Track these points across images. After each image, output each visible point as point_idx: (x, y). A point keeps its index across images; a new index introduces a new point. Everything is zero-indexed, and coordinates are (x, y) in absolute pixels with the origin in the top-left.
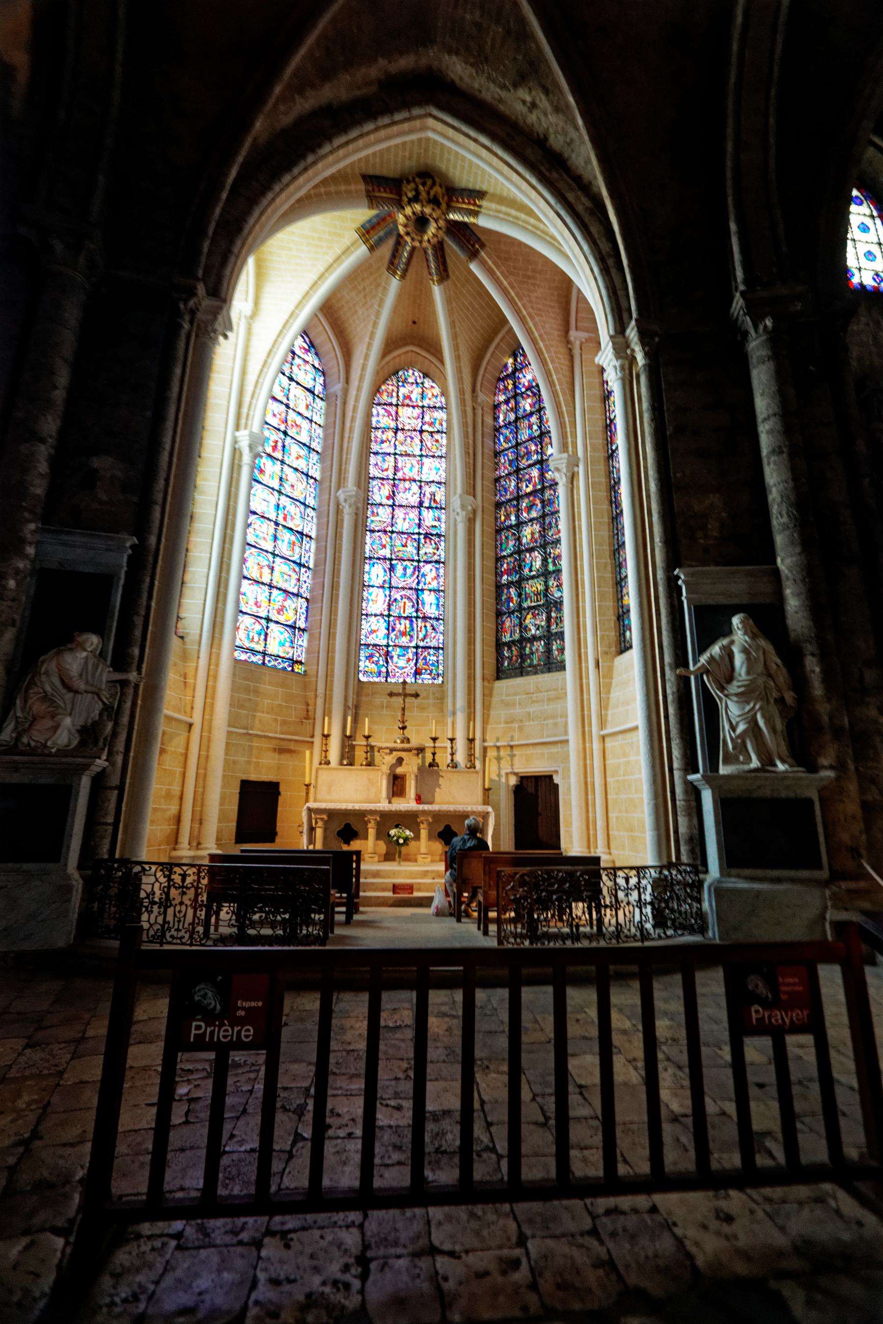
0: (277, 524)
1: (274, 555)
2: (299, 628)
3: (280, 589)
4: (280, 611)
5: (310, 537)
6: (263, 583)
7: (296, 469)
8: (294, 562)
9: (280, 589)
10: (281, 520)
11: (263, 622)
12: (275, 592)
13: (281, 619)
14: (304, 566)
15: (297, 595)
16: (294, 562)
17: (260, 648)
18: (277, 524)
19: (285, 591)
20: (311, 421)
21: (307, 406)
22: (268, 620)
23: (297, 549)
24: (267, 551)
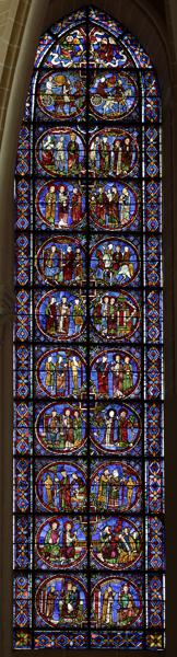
0: (88, 401)
1: (88, 458)
2: (151, 571)
3: (107, 514)
4: (111, 549)
5: (158, 401)
6: (72, 514)
7: (116, 288)
8: (129, 458)
9: (107, 514)
10: (94, 392)
11: (83, 578)
12: (98, 523)
13: (111, 563)
14: (150, 458)
15: (141, 514)
16: (129, 458)
17: (80, 621)
18: (88, 401)
19: (120, 516)
20: (138, 181)
21: (127, 158)
22: (89, 572)
23: (132, 434)
24: (74, 457)
